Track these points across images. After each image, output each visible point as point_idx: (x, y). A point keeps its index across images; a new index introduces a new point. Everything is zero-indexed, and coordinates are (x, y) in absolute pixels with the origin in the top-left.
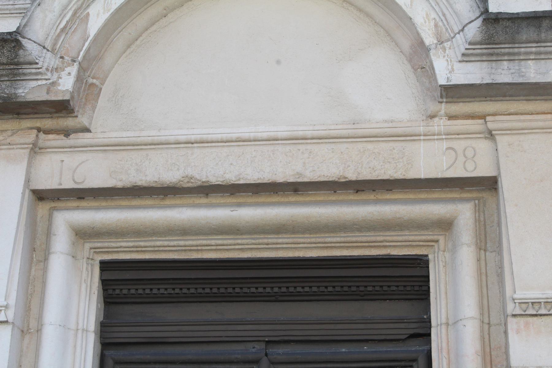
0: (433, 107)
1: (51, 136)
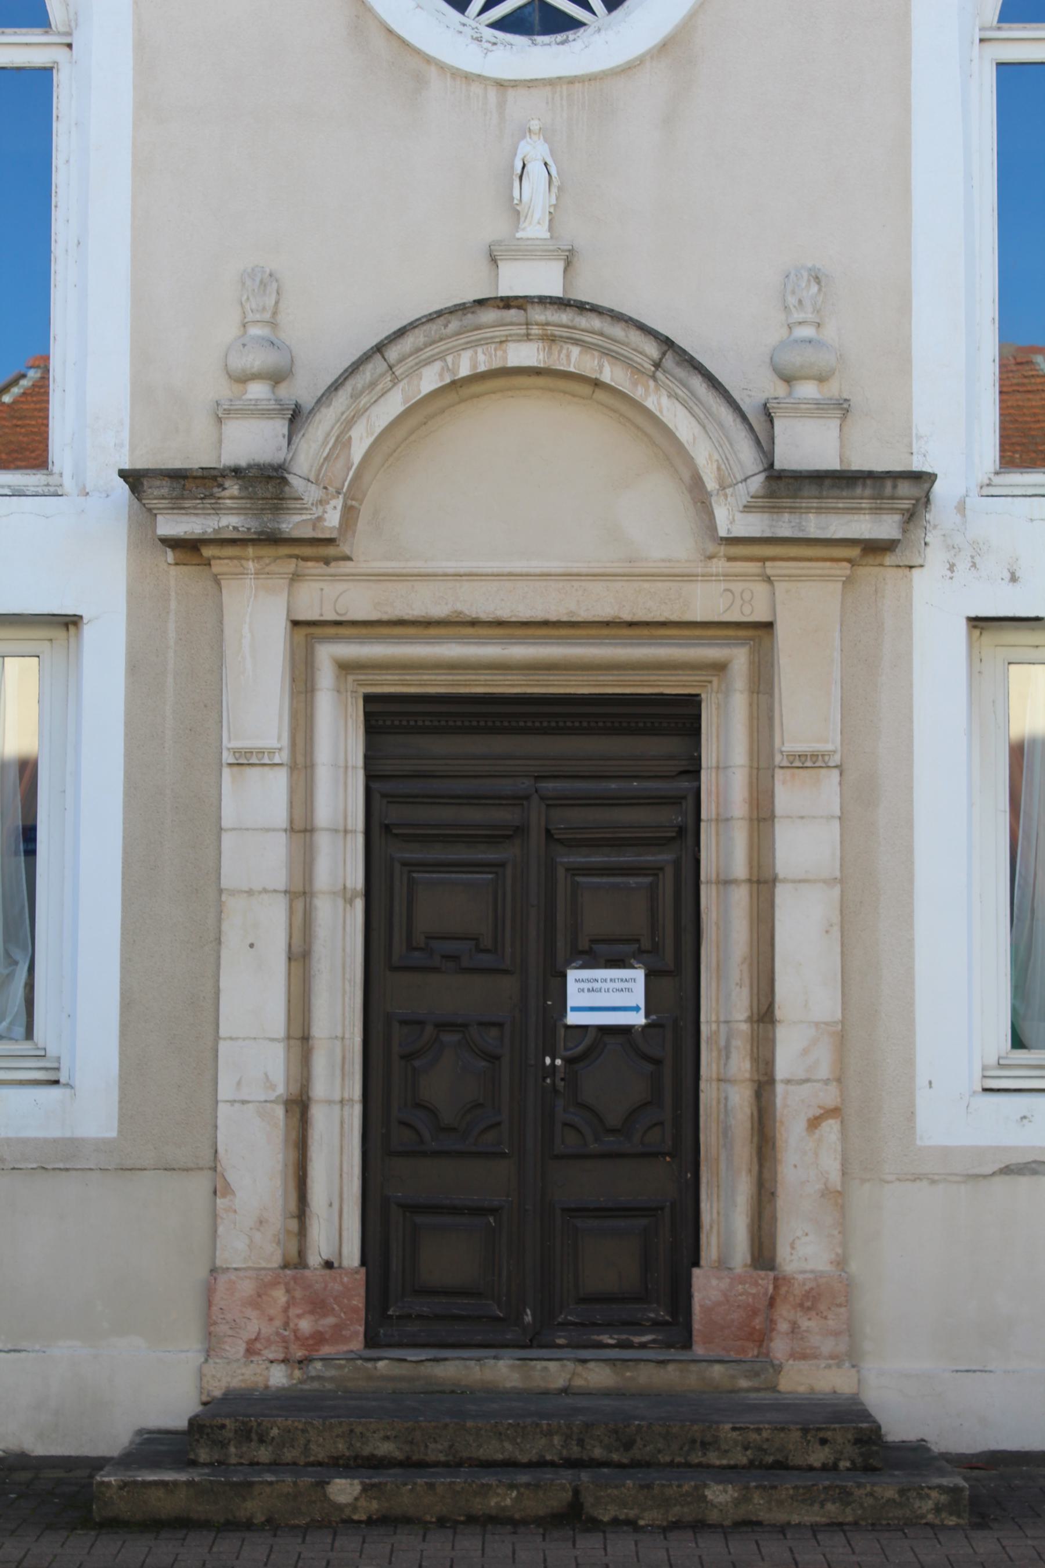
0: (711, 548)
1: (310, 564)
